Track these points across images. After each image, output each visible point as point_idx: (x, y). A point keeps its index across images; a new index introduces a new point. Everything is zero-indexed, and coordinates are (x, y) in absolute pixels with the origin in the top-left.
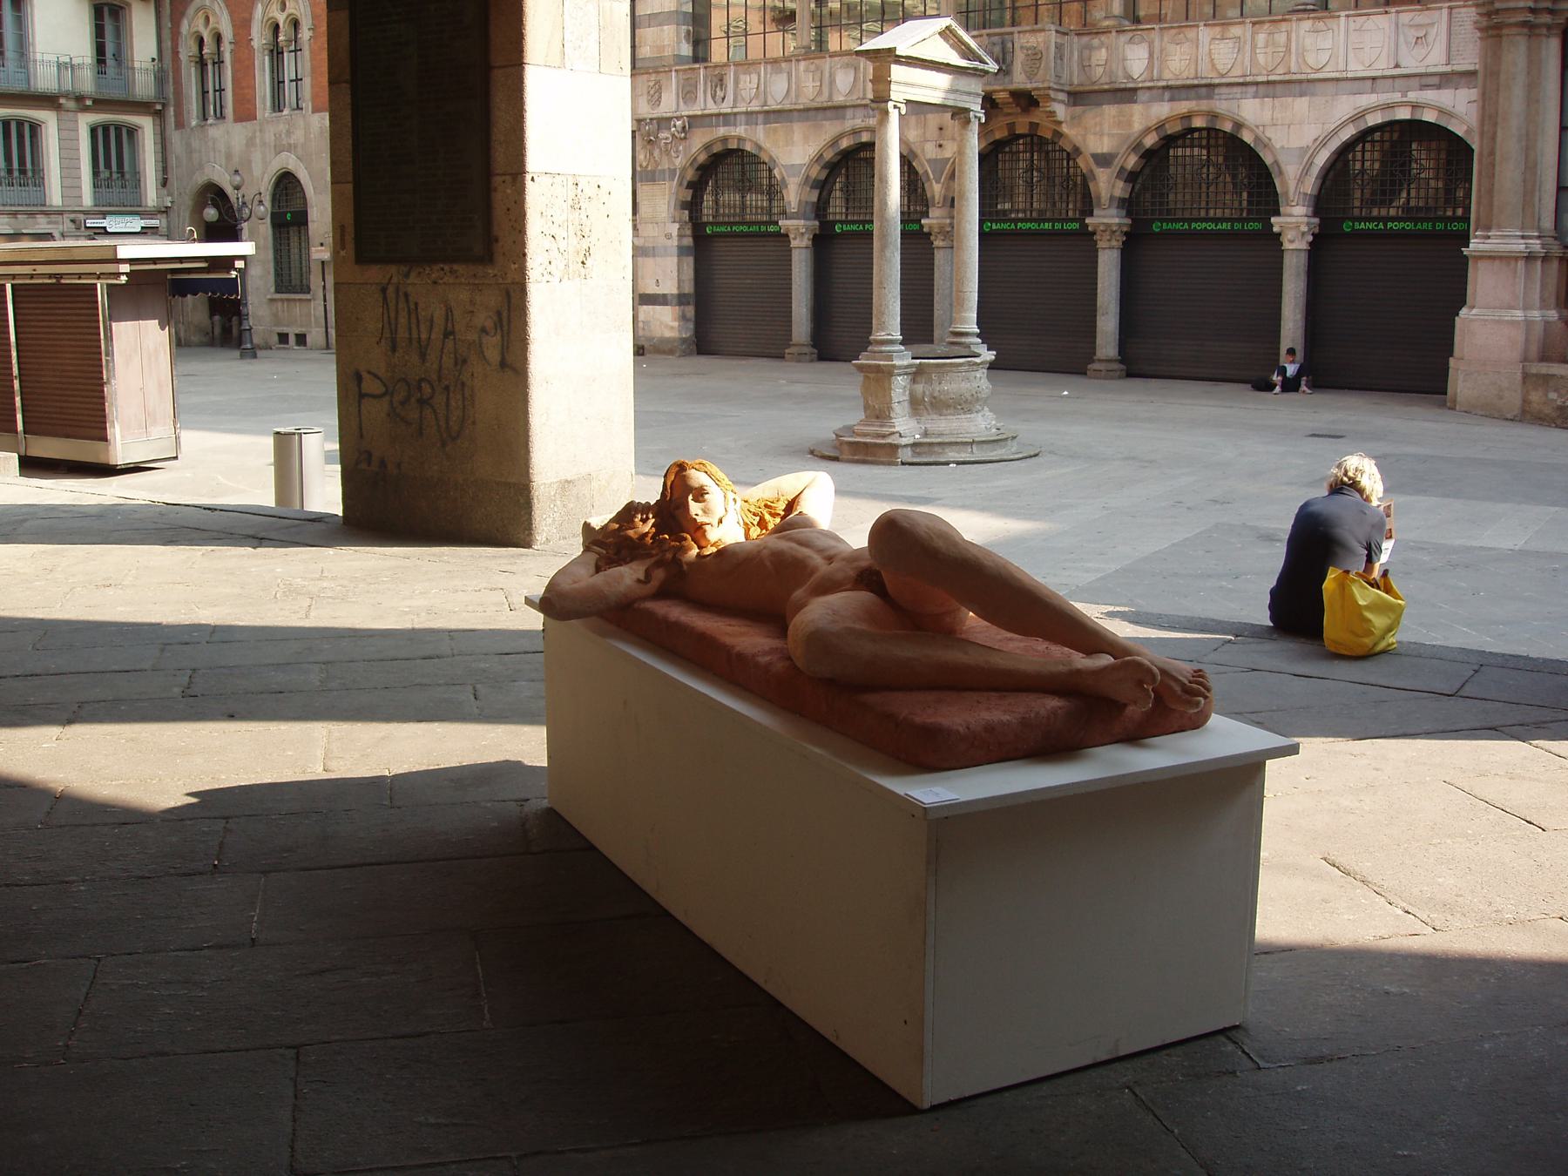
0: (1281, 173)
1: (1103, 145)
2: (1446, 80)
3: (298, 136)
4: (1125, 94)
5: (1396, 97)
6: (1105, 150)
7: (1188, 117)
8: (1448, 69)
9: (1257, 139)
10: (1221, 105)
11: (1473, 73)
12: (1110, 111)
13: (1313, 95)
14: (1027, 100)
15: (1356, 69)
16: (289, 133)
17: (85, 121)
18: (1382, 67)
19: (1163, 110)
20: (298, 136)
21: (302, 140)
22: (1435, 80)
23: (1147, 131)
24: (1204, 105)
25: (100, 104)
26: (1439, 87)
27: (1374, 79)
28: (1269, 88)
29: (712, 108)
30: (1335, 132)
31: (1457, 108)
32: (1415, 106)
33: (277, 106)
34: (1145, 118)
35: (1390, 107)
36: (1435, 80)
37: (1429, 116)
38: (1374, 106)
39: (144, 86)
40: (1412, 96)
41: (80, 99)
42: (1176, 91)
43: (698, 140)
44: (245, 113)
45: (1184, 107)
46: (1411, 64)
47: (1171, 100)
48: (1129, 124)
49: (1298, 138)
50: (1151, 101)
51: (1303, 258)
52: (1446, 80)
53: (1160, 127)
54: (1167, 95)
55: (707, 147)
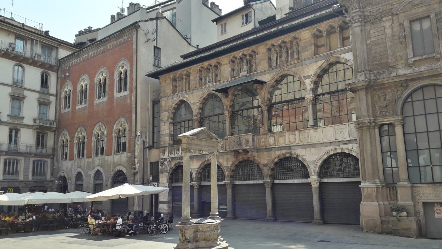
0: (309, 167)
1: (265, 162)
2: (349, 142)
3: (82, 164)
6: (265, 163)
7: (285, 154)
8: (350, 139)
9: (302, 159)
10: (293, 151)
11: (356, 140)
12: (266, 153)
13: (315, 147)
14: (246, 152)
15: (326, 140)
16: (80, 163)
17: (32, 159)
18: (333, 139)
19: (278, 153)
20: (82, 164)
21: (83, 164)
22: (347, 142)
23: (275, 158)
25: (36, 155)
26: (348, 144)
27: (330, 143)
28: (304, 146)
29: (176, 155)
30: (322, 157)
31: (353, 149)
32: (342, 149)
33: (79, 156)
35: (336, 149)
37: (346, 151)
38: (331, 150)
39: (49, 151)
40: (341, 146)
41: (30, 154)
42: (281, 148)
43: (173, 163)
44: (71, 159)
45: (283, 152)
46: (340, 139)
48: (271, 156)
49: (313, 158)
50: (276, 150)
51: (317, 190)
52: (349, 142)
53: (278, 157)
55: (175, 165)
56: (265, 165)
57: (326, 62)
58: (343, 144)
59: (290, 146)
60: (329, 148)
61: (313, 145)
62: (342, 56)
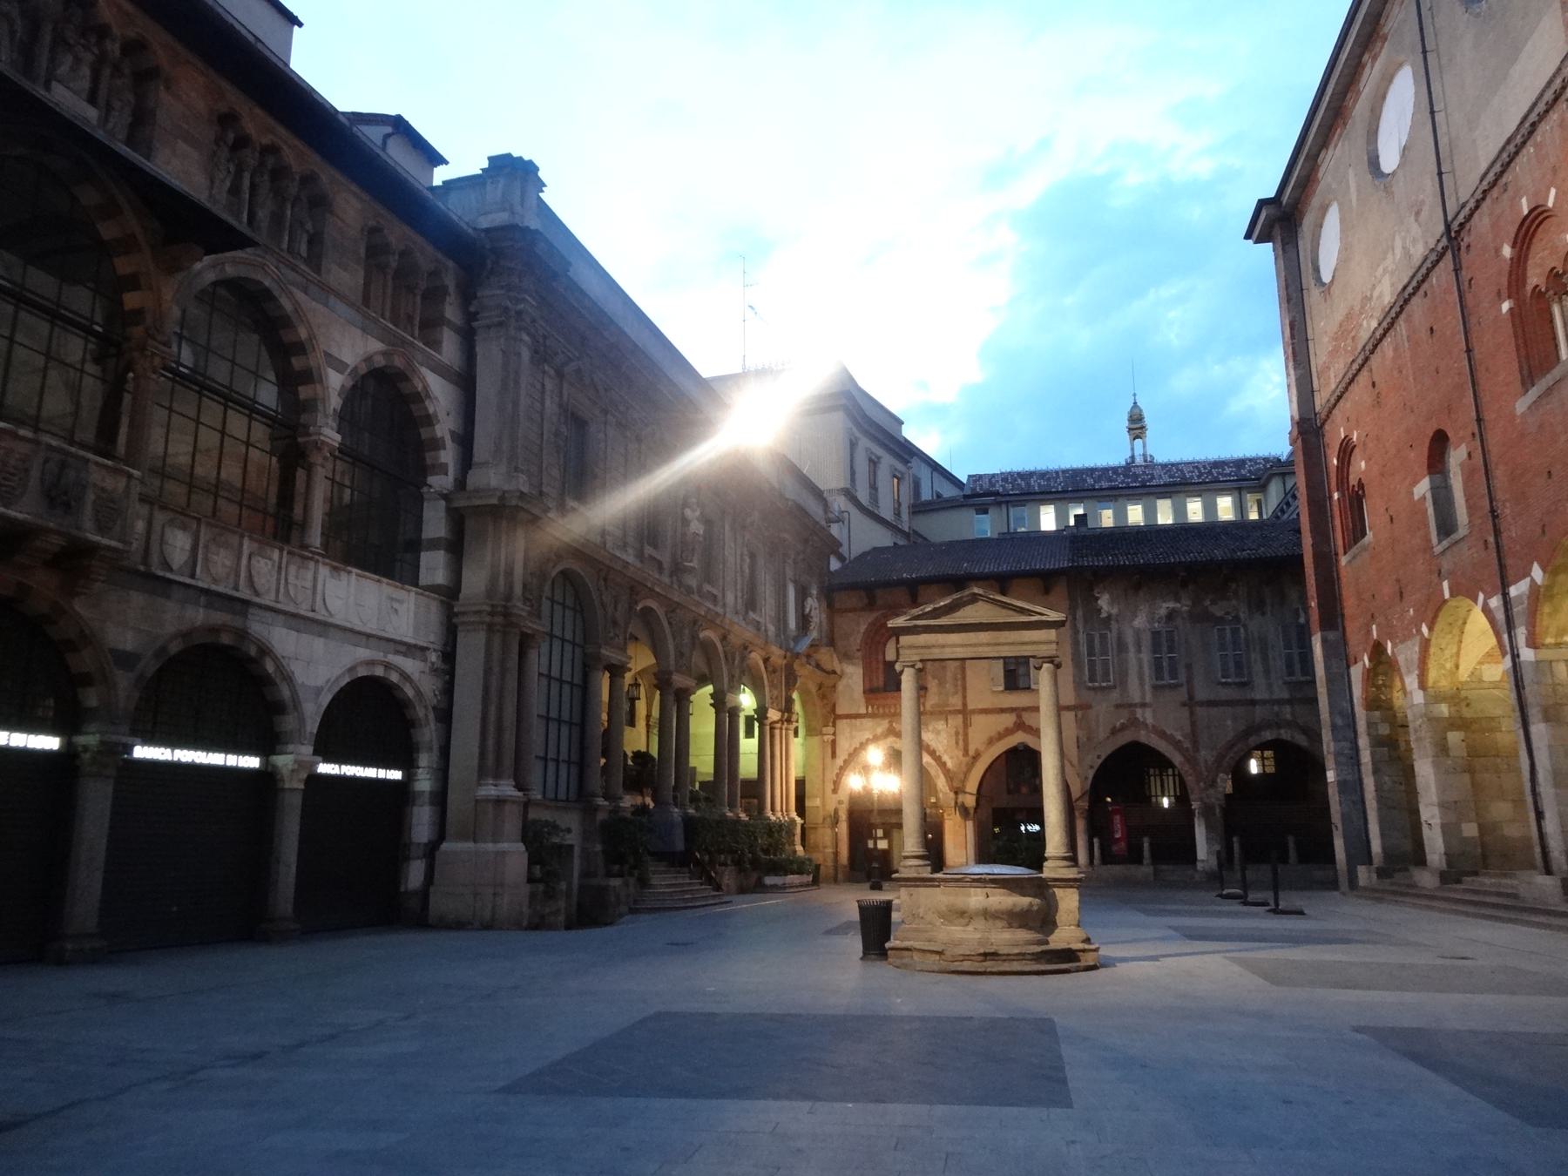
1: (127, 641)
2: (409, 649)
4: (159, 585)
5: (379, 656)
6: (129, 647)
7: (215, 630)
10: (257, 627)
11: (424, 649)
12: (137, 599)
19: (198, 615)
24: (237, 622)
26: (405, 655)
31: (416, 676)
32: (388, 666)
34: (179, 618)
36: (403, 649)
47: (208, 606)
52: (409, 649)
53: (185, 635)
54: (203, 599)
56: (126, 660)
57: (384, 354)
58: (397, 652)
59: (246, 603)
60: (363, 653)
61: (323, 627)
62: (425, 371)
